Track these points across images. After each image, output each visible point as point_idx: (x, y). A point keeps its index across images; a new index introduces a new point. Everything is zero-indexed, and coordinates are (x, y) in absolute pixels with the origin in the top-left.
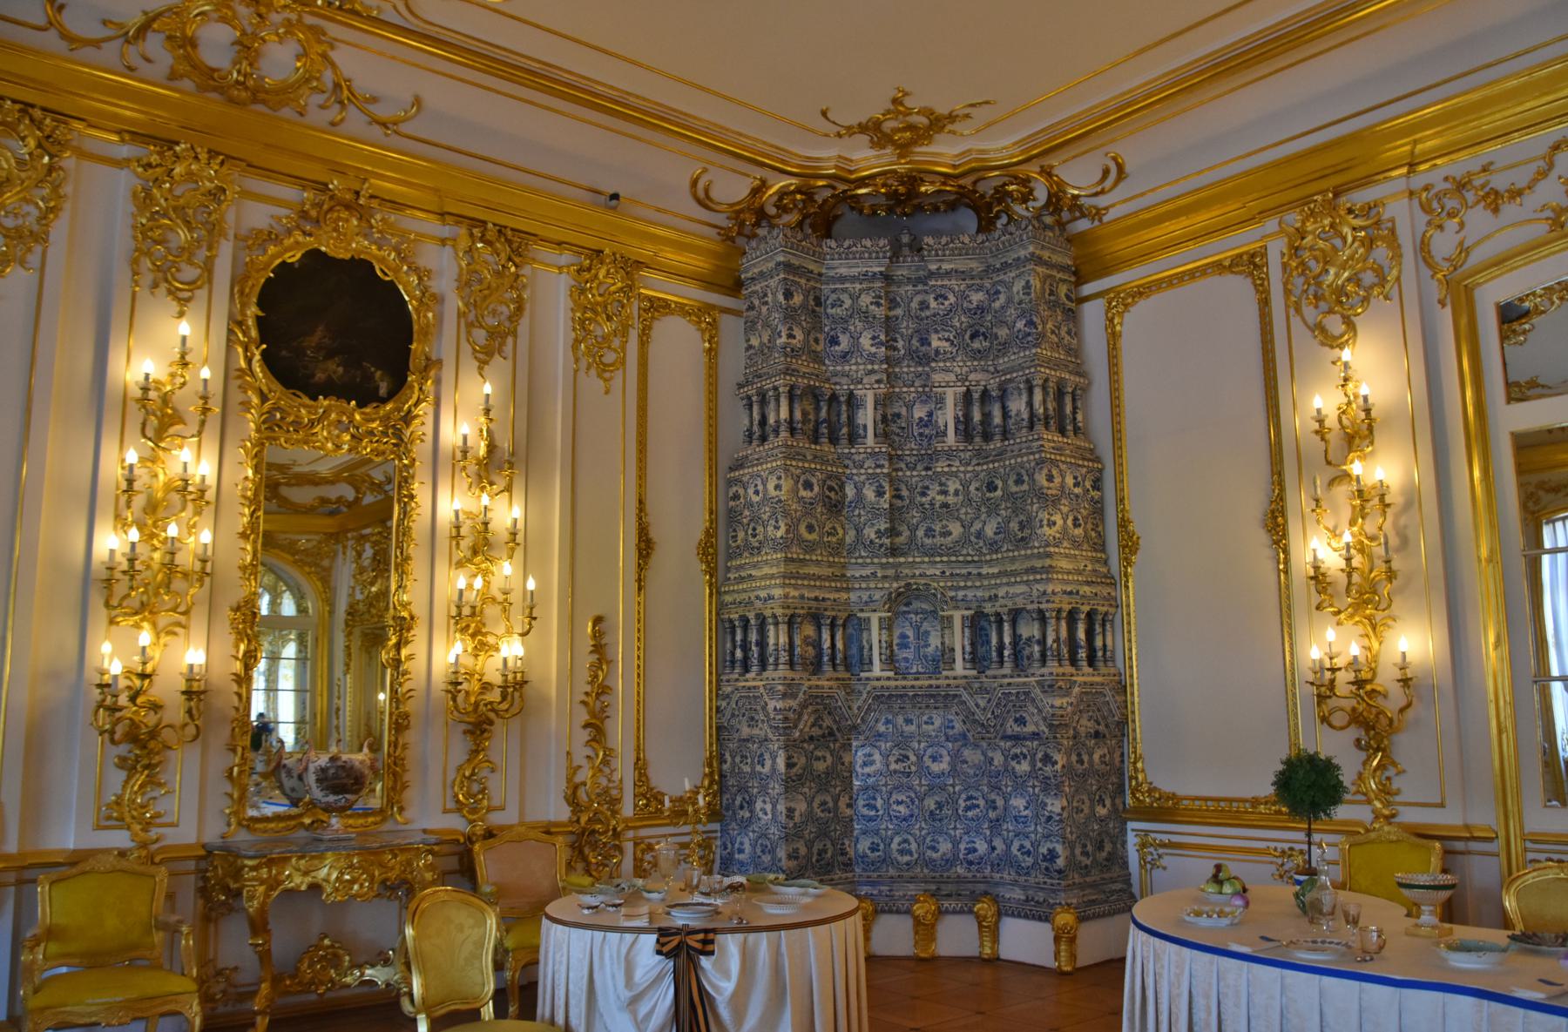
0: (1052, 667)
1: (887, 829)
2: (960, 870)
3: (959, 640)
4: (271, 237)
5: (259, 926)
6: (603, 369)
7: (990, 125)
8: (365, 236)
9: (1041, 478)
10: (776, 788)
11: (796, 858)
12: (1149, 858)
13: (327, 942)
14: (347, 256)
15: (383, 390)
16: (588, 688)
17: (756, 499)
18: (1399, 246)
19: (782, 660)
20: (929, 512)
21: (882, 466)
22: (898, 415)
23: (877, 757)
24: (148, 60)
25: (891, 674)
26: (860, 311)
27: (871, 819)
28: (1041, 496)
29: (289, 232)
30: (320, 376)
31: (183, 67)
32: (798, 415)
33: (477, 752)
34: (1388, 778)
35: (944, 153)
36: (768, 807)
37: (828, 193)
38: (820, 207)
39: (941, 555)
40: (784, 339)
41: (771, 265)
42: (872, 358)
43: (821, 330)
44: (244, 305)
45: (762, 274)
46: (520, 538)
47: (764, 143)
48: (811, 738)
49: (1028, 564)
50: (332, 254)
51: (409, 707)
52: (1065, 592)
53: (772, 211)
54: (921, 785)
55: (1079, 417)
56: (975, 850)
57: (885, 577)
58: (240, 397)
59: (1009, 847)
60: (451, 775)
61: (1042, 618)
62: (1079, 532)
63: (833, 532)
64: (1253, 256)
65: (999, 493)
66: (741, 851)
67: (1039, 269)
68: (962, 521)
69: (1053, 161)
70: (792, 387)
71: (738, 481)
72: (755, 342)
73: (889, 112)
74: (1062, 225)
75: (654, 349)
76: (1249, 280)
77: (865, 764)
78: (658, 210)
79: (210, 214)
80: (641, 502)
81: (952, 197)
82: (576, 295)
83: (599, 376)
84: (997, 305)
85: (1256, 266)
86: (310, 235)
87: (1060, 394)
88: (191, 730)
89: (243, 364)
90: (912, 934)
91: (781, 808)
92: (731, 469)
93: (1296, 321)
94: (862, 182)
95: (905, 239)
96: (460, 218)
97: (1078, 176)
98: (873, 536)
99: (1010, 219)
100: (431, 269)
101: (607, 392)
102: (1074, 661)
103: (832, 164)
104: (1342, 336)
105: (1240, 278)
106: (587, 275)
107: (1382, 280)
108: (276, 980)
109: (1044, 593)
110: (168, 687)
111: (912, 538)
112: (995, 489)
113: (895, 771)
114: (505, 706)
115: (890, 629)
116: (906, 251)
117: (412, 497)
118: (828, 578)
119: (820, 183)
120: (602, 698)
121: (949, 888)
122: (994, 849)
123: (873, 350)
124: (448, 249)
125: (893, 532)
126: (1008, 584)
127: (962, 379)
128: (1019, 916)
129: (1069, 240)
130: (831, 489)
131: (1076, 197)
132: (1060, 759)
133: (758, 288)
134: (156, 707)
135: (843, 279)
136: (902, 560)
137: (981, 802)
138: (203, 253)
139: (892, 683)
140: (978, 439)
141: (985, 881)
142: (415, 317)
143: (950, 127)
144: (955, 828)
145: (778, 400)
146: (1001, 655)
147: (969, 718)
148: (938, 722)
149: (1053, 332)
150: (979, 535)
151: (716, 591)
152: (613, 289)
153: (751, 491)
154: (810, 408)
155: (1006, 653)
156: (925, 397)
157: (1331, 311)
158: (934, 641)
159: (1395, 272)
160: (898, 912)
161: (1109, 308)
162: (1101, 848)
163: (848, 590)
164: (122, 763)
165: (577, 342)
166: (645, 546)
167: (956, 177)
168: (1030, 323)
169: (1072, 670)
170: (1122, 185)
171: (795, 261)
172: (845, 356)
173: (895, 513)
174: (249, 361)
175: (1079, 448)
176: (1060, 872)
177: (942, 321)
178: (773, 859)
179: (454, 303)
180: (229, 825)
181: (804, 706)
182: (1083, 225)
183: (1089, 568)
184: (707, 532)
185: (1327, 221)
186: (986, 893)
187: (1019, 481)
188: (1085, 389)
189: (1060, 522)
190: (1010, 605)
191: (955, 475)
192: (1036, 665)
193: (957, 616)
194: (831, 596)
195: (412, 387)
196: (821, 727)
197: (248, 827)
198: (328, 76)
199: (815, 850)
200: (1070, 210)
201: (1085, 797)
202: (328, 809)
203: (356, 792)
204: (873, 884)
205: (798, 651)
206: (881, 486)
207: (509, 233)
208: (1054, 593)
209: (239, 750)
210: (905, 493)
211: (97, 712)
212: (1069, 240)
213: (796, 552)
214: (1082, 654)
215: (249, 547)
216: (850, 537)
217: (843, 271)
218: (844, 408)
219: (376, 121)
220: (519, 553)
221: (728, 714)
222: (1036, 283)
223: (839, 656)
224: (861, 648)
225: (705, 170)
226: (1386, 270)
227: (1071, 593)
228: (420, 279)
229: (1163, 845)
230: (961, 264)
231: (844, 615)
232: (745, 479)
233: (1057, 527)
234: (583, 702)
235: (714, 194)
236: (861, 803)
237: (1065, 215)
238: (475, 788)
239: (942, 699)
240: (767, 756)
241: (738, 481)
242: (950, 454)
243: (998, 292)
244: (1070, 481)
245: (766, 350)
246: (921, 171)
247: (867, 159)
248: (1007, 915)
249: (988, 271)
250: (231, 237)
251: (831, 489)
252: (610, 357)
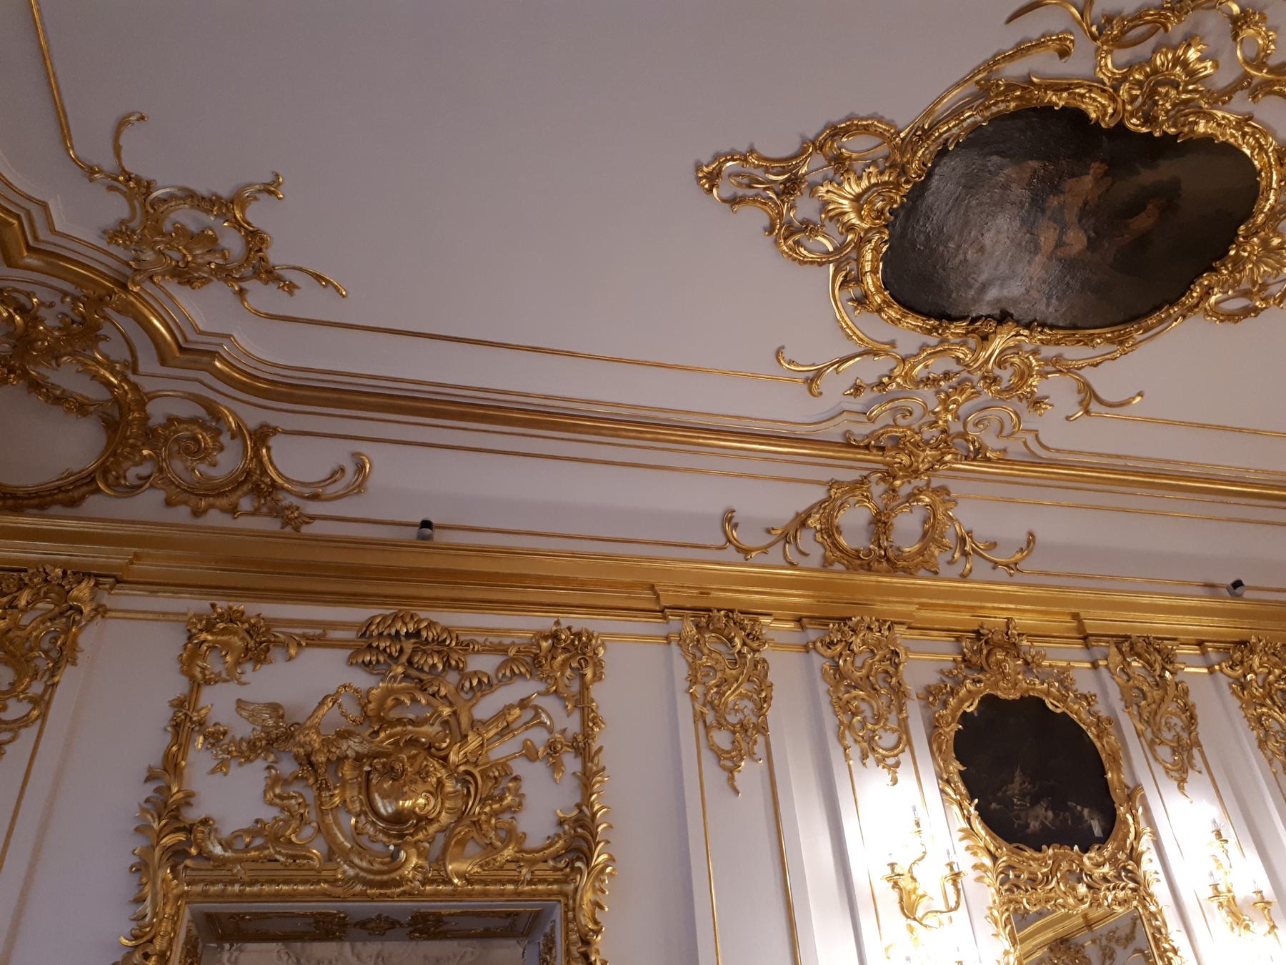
14: (1014, 695)
15: (1097, 831)
30: (1034, 825)
86: (980, 681)
89: (965, 825)
106: (1239, 671)
142: (1098, 745)
165: (1262, 744)
179: (1128, 724)
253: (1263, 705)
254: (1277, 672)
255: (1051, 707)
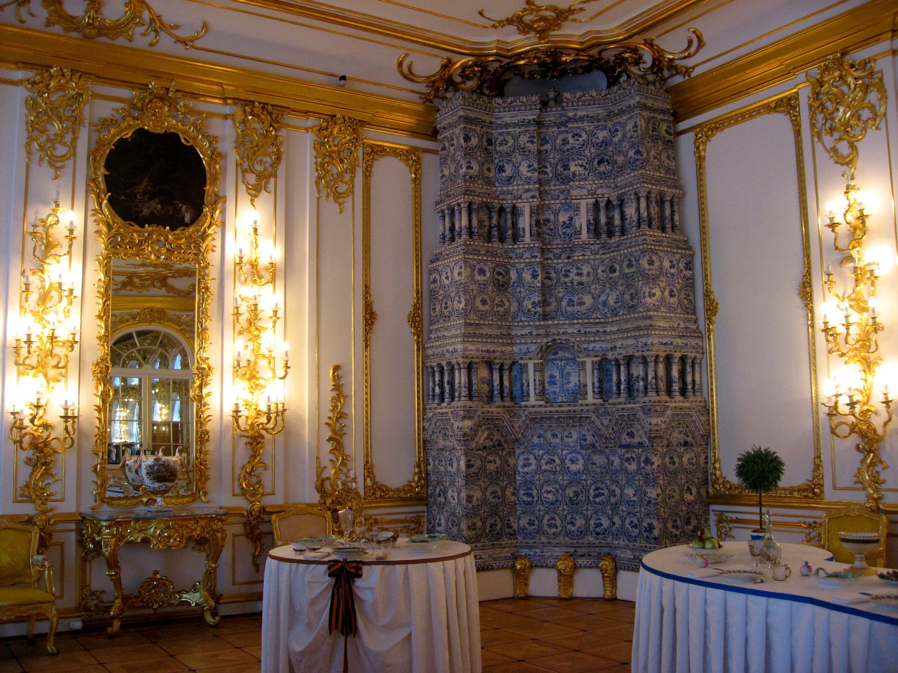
0: (652, 396)
1: (540, 510)
2: (591, 539)
3: (590, 378)
4: (113, 122)
5: (113, 563)
6: (338, 197)
7: (598, 14)
8: (174, 117)
9: (644, 263)
10: (460, 482)
11: (474, 529)
12: (724, 531)
13: (158, 576)
15: (187, 219)
16: (331, 415)
17: (447, 282)
18: (885, 91)
19: (463, 394)
20: (570, 289)
21: (535, 257)
22: (548, 220)
23: (533, 461)
24: (32, 15)
25: (542, 403)
26: (519, 148)
27: (529, 503)
28: (645, 276)
29: (124, 118)
30: (146, 211)
31: (55, 18)
32: (475, 223)
33: (254, 457)
34: (877, 472)
35: (573, 33)
36: (455, 495)
37: (497, 65)
38: (492, 74)
39: (578, 319)
40: (463, 171)
41: (455, 118)
42: (528, 181)
43: (492, 162)
44: (96, 169)
45: (450, 125)
46: (280, 314)
47: (445, 35)
48: (485, 448)
49: (636, 324)
50: (152, 131)
51: (208, 427)
52: (661, 344)
53: (458, 79)
54: (563, 480)
55: (676, 218)
56: (601, 525)
57: (538, 335)
58: (97, 228)
59: (623, 522)
60: (238, 471)
61: (645, 362)
62: (672, 300)
63: (501, 304)
64: (790, 99)
65: (617, 273)
66: (439, 525)
67: (646, 114)
68: (592, 294)
69: (651, 35)
70: (470, 205)
71: (435, 270)
72: (446, 172)
73: (525, 10)
74: (664, 80)
75: (374, 181)
76: (788, 116)
77: (525, 466)
78: (376, 84)
79: (73, 111)
80: (366, 287)
81: (587, 63)
82: (318, 146)
83: (335, 201)
84: (616, 139)
85: (791, 106)
86: (138, 119)
87: (661, 202)
88: (69, 441)
90: (557, 582)
91: (463, 495)
92: (432, 262)
93: (818, 146)
94: (520, 56)
95: (552, 95)
96: (236, 101)
97: (672, 44)
98: (530, 306)
99: (629, 77)
100: (220, 133)
101: (341, 212)
102: (669, 392)
103: (494, 45)
104: (848, 156)
105: (781, 115)
106: (325, 133)
107: (875, 116)
108: (125, 599)
109: (646, 344)
110: (54, 415)
111: (559, 307)
112: (615, 271)
113: (546, 471)
114: (271, 425)
115: (542, 371)
116: (552, 103)
117: (207, 289)
118: (497, 337)
119: (491, 59)
120: (341, 421)
121: (581, 551)
122: (614, 524)
123: (529, 174)
124: (229, 122)
125: (545, 303)
126: (622, 338)
127: (592, 193)
128: (628, 570)
129: (667, 91)
130: (499, 274)
131: (671, 60)
132: (656, 461)
133: (447, 134)
134: (46, 426)
135: (507, 125)
136: (550, 322)
137: (606, 492)
138: (68, 138)
139: (543, 409)
140: (604, 236)
141: (608, 546)
142: (207, 168)
143: (571, 17)
144: (587, 510)
145: (460, 213)
146: (619, 388)
147: (597, 433)
148: (575, 436)
149: (655, 158)
150: (605, 304)
151: (421, 346)
152: (343, 141)
153: (444, 277)
154: (485, 218)
155: (622, 387)
156: (568, 206)
157: (840, 139)
158: (574, 380)
159: (883, 110)
160: (547, 567)
161: (697, 139)
162: (688, 523)
163: (512, 344)
164: (28, 461)
165: (319, 179)
166: (370, 317)
167: (583, 50)
168: (638, 152)
169: (667, 398)
170: (702, 51)
171: (472, 115)
172: (509, 180)
173: (546, 290)
174: (100, 205)
175: (675, 240)
176: (655, 539)
177: (578, 152)
178: (459, 530)
179: (233, 157)
180: (96, 501)
181: (479, 425)
182: (678, 79)
183: (682, 325)
184: (415, 306)
185: (837, 74)
186: (609, 554)
187: (630, 265)
188: (682, 197)
189: (658, 294)
190: (624, 352)
191: (587, 261)
192: (641, 395)
193: (589, 362)
194: (500, 349)
195: (206, 216)
196: (492, 440)
197: (107, 503)
198: (146, 15)
199: (488, 524)
200: (668, 69)
201: (676, 487)
202: (155, 492)
203: (172, 481)
204: (530, 547)
205: (475, 387)
206: (535, 271)
207: (270, 108)
208: (652, 344)
209: (100, 454)
210: (553, 275)
211: (12, 429)
212: (667, 91)
213: (473, 318)
214: (676, 387)
215: (103, 325)
216: (514, 307)
217: (507, 120)
218: (509, 216)
219: (178, 40)
220: (280, 324)
221: (430, 432)
222: (642, 123)
223: (506, 391)
224: (522, 385)
225: (407, 55)
226: (877, 108)
227: (666, 344)
228: (210, 143)
229: (732, 521)
230: (592, 111)
231: (509, 362)
232: (440, 269)
233: (655, 298)
234: (327, 424)
235: (414, 71)
236: (522, 492)
237: (666, 73)
238: (254, 480)
239: (578, 419)
240: (454, 460)
241: (435, 270)
242: (584, 247)
243: (616, 130)
244: (666, 264)
245: (452, 178)
246: (556, 48)
247: (518, 41)
248: (621, 569)
249: (610, 116)
250: (87, 125)
251: (499, 274)
252: (343, 188)
253: (330, 156)
254: (348, 138)
255: (183, 141)
